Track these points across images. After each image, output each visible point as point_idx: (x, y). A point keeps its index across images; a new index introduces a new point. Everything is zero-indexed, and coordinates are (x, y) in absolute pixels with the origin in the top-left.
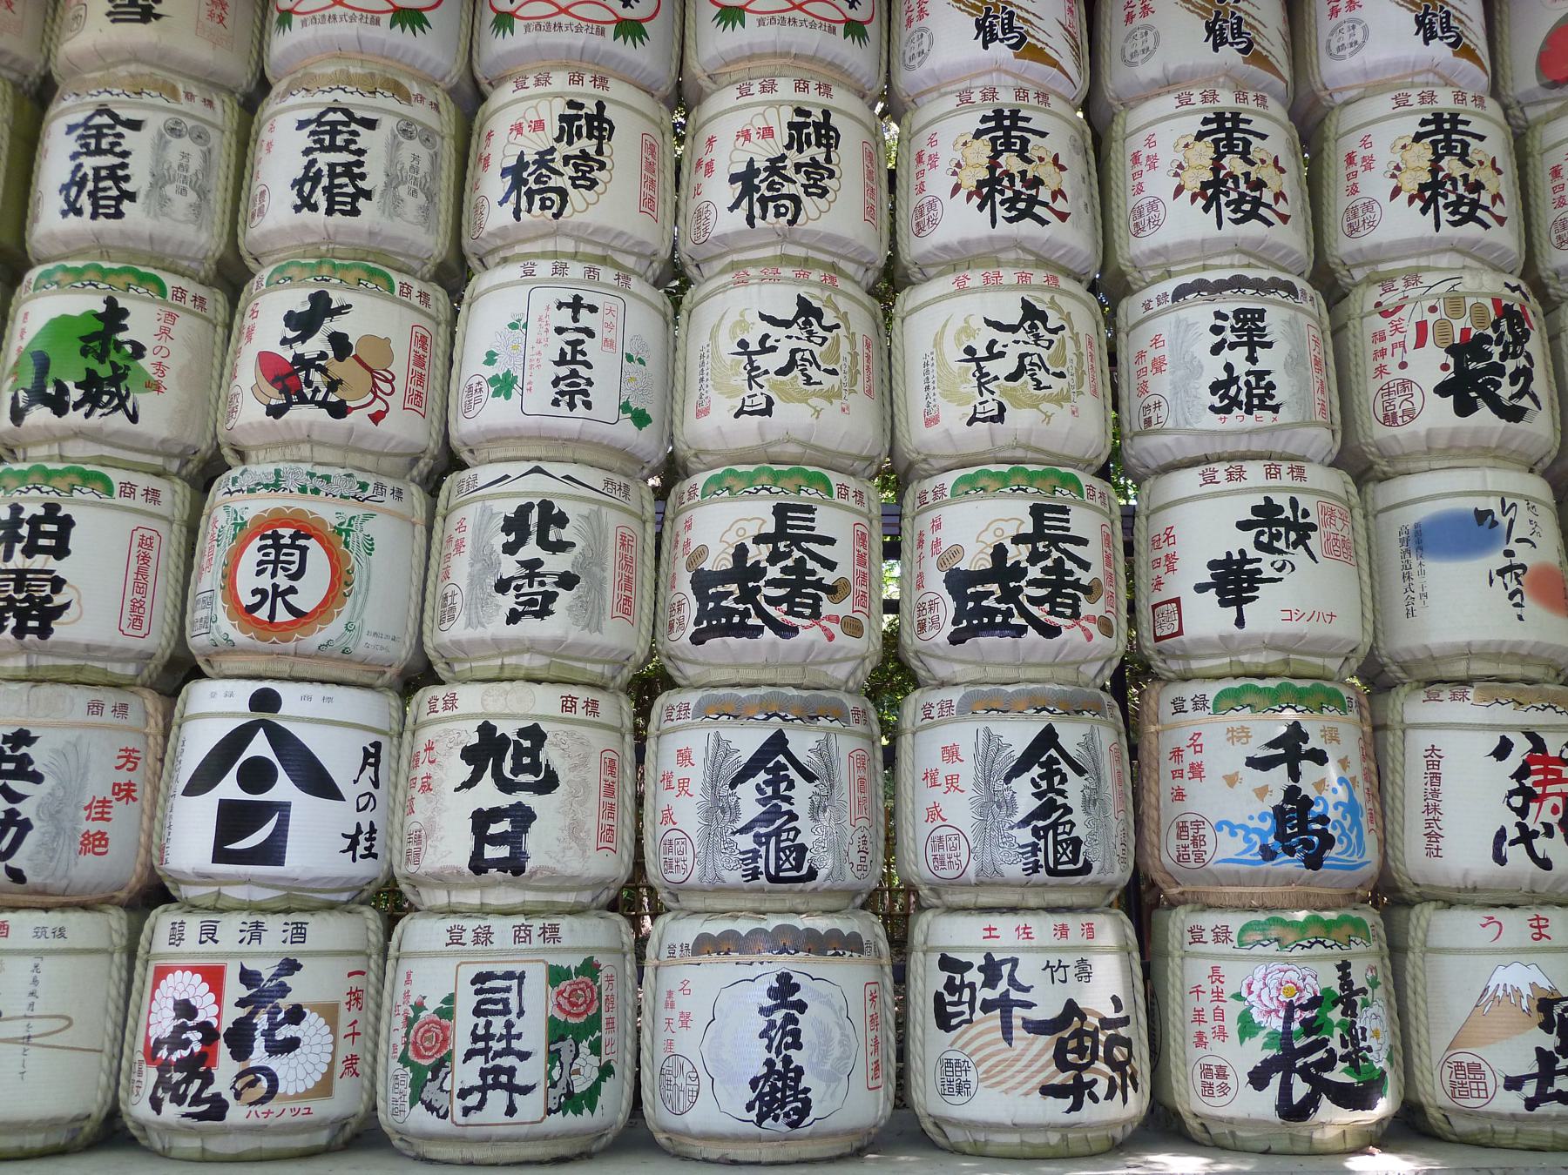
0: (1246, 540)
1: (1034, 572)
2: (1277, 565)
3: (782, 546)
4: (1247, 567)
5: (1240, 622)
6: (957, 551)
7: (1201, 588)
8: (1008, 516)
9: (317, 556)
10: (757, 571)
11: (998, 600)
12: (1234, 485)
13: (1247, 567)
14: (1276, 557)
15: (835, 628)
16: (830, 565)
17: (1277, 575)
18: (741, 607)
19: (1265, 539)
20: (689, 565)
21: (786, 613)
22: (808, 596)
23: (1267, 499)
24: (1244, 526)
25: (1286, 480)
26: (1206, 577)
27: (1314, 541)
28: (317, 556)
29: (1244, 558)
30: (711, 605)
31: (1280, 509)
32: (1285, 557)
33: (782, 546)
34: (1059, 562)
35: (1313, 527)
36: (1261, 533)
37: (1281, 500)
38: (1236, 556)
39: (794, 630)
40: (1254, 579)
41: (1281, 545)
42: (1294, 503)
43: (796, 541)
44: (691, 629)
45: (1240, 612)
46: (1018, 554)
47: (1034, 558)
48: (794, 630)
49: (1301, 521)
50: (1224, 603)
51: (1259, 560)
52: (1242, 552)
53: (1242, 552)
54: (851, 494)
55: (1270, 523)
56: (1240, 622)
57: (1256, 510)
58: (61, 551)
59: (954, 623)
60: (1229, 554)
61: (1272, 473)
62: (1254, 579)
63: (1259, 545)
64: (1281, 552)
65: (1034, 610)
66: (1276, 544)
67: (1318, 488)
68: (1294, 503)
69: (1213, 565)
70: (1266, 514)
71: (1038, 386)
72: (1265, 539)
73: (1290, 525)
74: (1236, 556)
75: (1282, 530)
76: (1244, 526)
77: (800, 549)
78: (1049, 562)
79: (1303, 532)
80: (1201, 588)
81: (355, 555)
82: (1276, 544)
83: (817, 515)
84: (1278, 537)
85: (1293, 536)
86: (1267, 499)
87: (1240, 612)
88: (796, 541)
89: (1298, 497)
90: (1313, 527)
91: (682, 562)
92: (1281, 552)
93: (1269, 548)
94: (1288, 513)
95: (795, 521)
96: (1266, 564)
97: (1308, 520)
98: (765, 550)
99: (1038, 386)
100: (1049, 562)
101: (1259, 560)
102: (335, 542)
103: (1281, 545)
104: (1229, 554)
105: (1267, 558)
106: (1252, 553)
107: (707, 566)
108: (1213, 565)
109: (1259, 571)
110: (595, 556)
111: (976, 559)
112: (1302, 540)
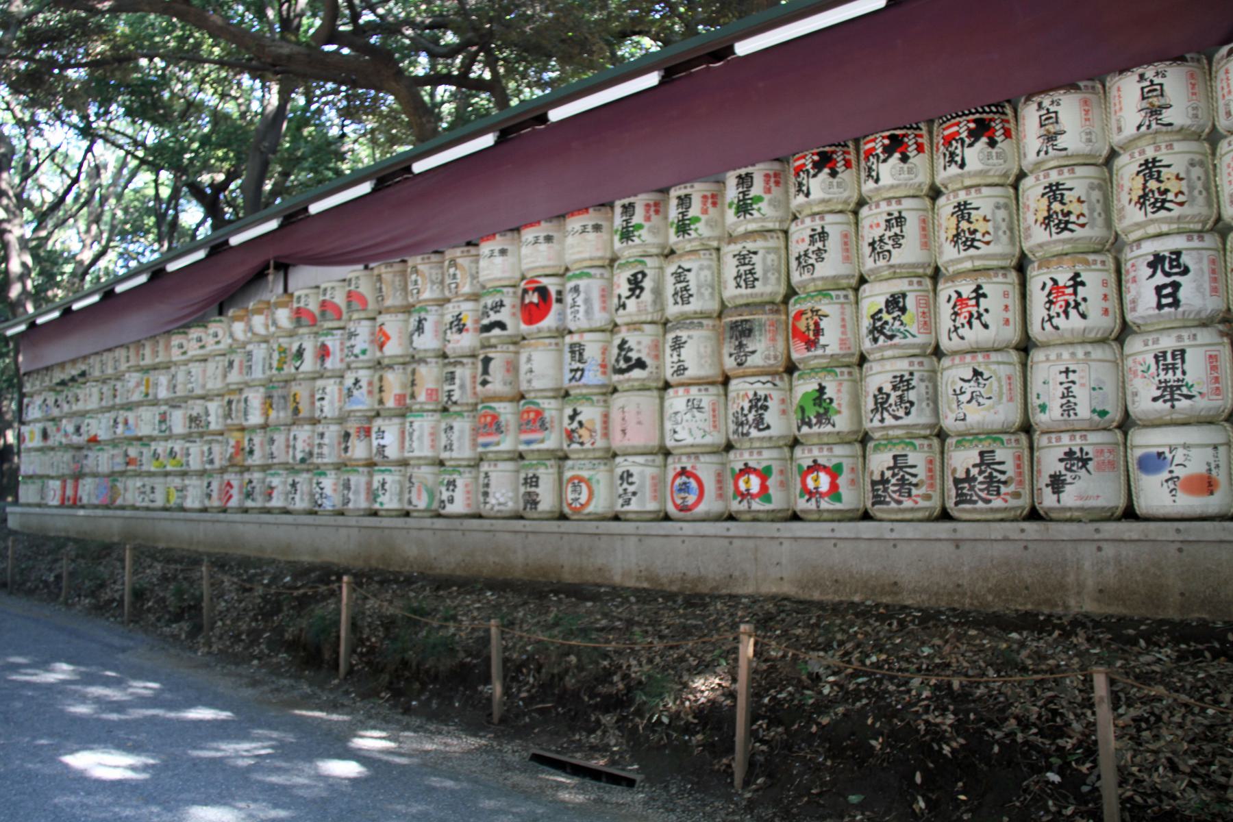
1: (980, 479)
5: (1059, 501)
9: (584, 486)
24: (1061, 460)
25: (1078, 441)
27: (1090, 465)
28: (584, 486)
29: (1060, 475)
35: (1090, 459)
40: (1064, 482)
41: (1074, 468)
42: (1081, 450)
43: (901, 468)
55: (1070, 459)
56: (1059, 501)
57: (1066, 454)
58: (537, 486)
61: (1073, 438)
62: (1064, 482)
63: (1066, 469)
68: (1081, 450)
69: (1051, 476)
70: (1070, 454)
71: (979, 404)
73: (1079, 459)
76: (1061, 460)
79: (1085, 462)
81: (595, 486)
88: (901, 468)
90: (1090, 459)
94: (1078, 454)
95: (900, 462)
96: (1068, 477)
99: (979, 404)
102: (588, 481)
106: (1064, 472)
108: (1051, 476)
110: (642, 486)
111: (961, 474)
112: (1084, 466)
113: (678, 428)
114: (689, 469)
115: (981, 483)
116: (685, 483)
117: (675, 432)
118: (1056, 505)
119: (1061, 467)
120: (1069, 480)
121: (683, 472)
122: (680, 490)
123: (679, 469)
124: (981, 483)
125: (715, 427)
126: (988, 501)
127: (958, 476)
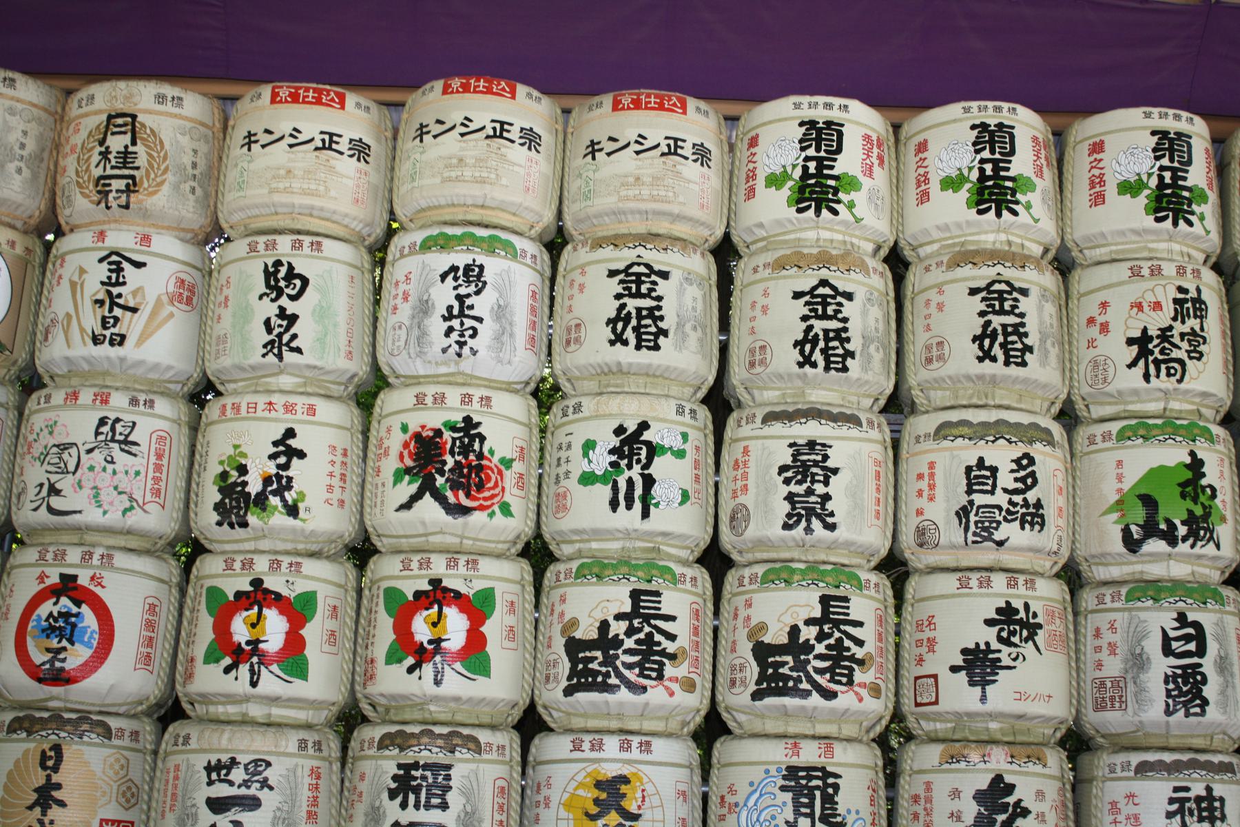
0: (990, 634)
1: (820, 648)
2: (1013, 656)
3: (636, 623)
4: (991, 656)
5: (983, 698)
6: (762, 627)
7: (955, 669)
8: (803, 603)
10: (616, 642)
11: (791, 669)
12: (983, 590)
13: (991, 656)
14: (1012, 649)
15: (675, 687)
16: (672, 637)
17: (1012, 664)
18: (604, 669)
19: (1004, 634)
20: (563, 632)
21: (638, 676)
22: (655, 662)
23: (1008, 603)
24: (989, 623)
25: (1022, 590)
26: (959, 661)
27: (1040, 637)
30: (581, 666)
31: (1017, 611)
32: (1018, 650)
33: (636, 623)
34: (840, 640)
35: (1040, 626)
36: (1002, 630)
37: (1018, 604)
38: (983, 647)
39: (644, 689)
40: (996, 665)
41: (1016, 640)
42: (1027, 606)
44: (565, 683)
45: (984, 691)
46: (808, 633)
47: (821, 637)
48: (644, 689)
49: (1031, 621)
50: (972, 683)
51: (999, 651)
52: (987, 644)
53: (987, 644)
54: (688, 580)
55: (1009, 622)
56: (983, 698)
57: (999, 611)
59: (757, 684)
60: (977, 644)
61: (1012, 584)
62: (996, 665)
63: (1000, 639)
64: (1016, 646)
65: (817, 677)
66: (1012, 639)
67: (1045, 596)
68: (1027, 606)
70: (1006, 614)
72: (1004, 634)
73: (1024, 624)
74: (983, 647)
75: (1018, 628)
76: (989, 623)
77: (650, 625)
78: (832, 641)
80: (955, 669)
82: (1012, 639)
83: (662, 599)
84: (1013, 633)
85: (1025, 633)
86: (1008, 603)
87: (984, 691)
89: (1030, 602)
90: (1040, 626)
91: (557, 628)
92: (1016, 646)
93: (1007, 642)
94: (1022, 614)
96: (1005, 655)
97: (1036, 621)
98: (622, 626)
100: (832, 641)
101: (999, 651)
103: (1016, 640)
104: (977, 644)
105: (1006, 650)
106: (995, 645)
107: (578, 635)
108: (965, 651)
109: (999, 660)
111: (776, 635)
112: (1031, 637)
113: (65, 483)
114: (84, 580)
115: (820, 657)
116: (66, 615)
117: (54, 491)
118: (977, 706)
119: (989, 635)
120: (1006, 661)
121: (67, 586)
122: (50, 631)
123: (54, 579)
124: (820, 657)
125: (157, 493)
126: (829, 695)
127: (767, 639)
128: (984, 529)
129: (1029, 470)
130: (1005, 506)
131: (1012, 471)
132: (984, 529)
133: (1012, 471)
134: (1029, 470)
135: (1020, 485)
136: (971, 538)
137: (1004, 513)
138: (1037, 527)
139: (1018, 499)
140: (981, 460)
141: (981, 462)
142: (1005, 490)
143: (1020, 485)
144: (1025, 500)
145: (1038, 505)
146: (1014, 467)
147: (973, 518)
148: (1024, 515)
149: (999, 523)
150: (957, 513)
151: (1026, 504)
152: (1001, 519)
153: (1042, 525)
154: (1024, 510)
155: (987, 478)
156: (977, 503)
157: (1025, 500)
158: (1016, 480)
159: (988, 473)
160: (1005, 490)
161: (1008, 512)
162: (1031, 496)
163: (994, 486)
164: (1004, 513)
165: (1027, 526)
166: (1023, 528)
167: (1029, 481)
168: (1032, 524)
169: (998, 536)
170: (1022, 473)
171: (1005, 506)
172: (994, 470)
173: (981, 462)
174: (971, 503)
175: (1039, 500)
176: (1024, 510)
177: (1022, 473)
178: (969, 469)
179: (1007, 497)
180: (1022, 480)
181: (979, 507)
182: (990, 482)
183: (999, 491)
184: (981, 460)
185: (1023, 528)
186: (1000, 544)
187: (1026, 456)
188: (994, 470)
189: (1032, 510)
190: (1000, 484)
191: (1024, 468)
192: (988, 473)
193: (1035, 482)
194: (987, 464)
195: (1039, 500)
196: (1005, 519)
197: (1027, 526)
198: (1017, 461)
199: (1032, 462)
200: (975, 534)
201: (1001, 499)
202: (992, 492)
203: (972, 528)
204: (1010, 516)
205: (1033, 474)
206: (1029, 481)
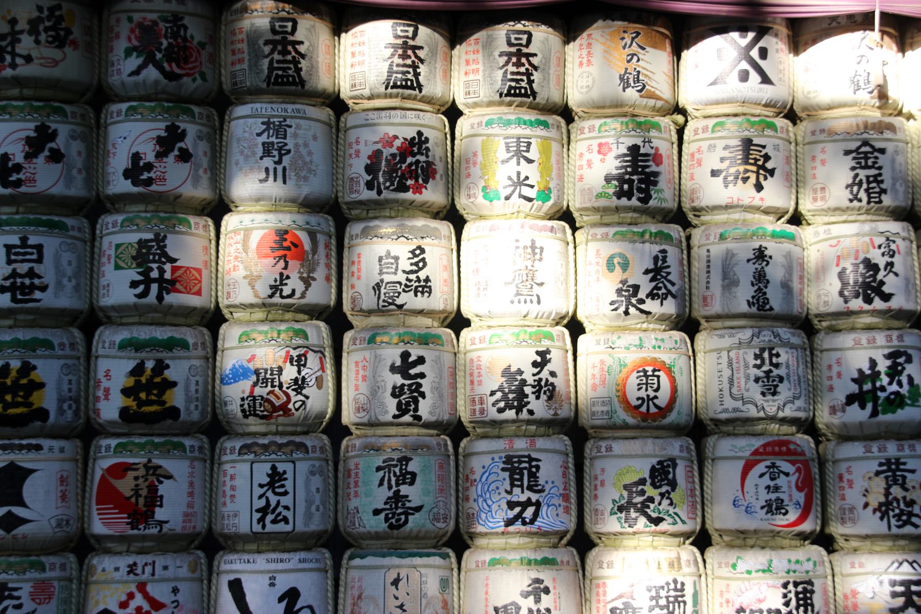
128: (389, 298)
129: (421, 257)
130: (404, 282)
131: (409, 259)
132: (389, 298)
133: (409, 259)
134: (421, 257)
135: (414, 268)
136: (381, 303)
137: (403, 287)
138: (426, 294)
139: (413, 277)
140: (388, 253)
141: (388, 254)
142: (404, 271)
143: (414, 268)
144: (418, 277)
145: (427, 280)
146: (411, 256)
147: (383, 291)
148: (417, 287)
149: (399, 293)
150: (374, 288)
151: (418, 280)
152: (401, 290)
153: (430, 293)
154: (417, 284)
155: (392, 264)
156: (385, 281)
157: (418, 277)
158: (412, 264)
159: (393, 261)
160: (404, 271)
161: (406, 286)
162: (422, 275)
163: (397, 269)
164: (403, 287)
165: (419, 294)
166: (416, 295)
167: (421, 264)
168: (423, 293)
169: (399, 301)
170: (416, 260)
171: (404, 282)
172: (397, 258)
173: (388, 254)
174: (382, 281)
175: (428, 277)
176: (417, 284)
177: (416, 260)
178: (380, 259)
179: (405, 276)
180: (416, 264)
181: (388, 283)
182: (394, 266)
183: (400, 272)
184: (388, 253)
185: (416, 295)
186: (400, 307)
187: (419, 248)
188: (397, 258)
189: (422, 283)
190: (401, 268)
191: (417, 256)
192: (393, 261)
193: (425, 265)
194: (392, 254)
195: (428, 277)
196: (404, 291)
197: (419, 294)
198: (413, 252)
199: (423, 251)
200: (384, 301)
201: (401, 277)
202: (395, 273)
203: (382, 297)
204: (407, 288)
205: (423, 260)
206: (421, 264)
